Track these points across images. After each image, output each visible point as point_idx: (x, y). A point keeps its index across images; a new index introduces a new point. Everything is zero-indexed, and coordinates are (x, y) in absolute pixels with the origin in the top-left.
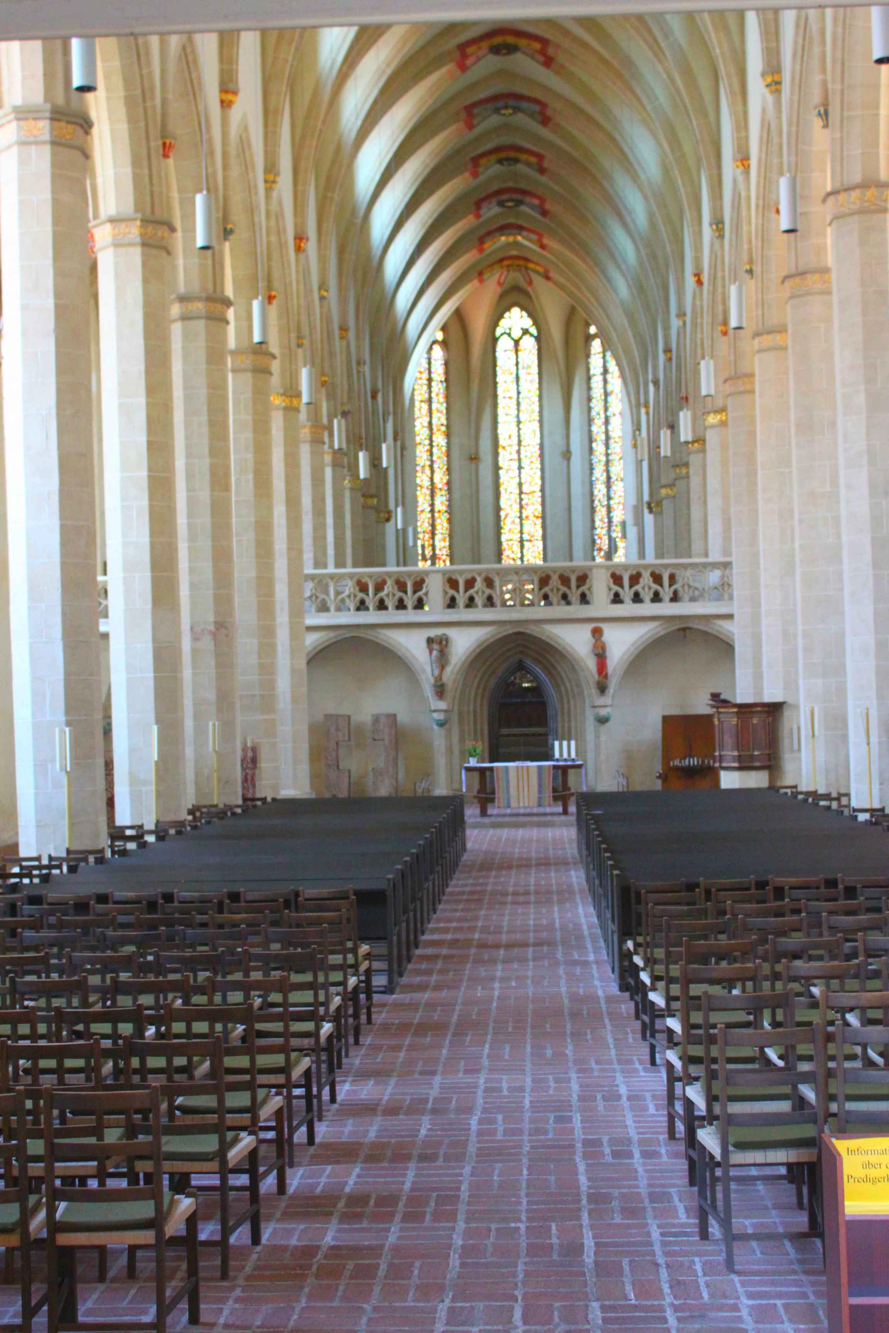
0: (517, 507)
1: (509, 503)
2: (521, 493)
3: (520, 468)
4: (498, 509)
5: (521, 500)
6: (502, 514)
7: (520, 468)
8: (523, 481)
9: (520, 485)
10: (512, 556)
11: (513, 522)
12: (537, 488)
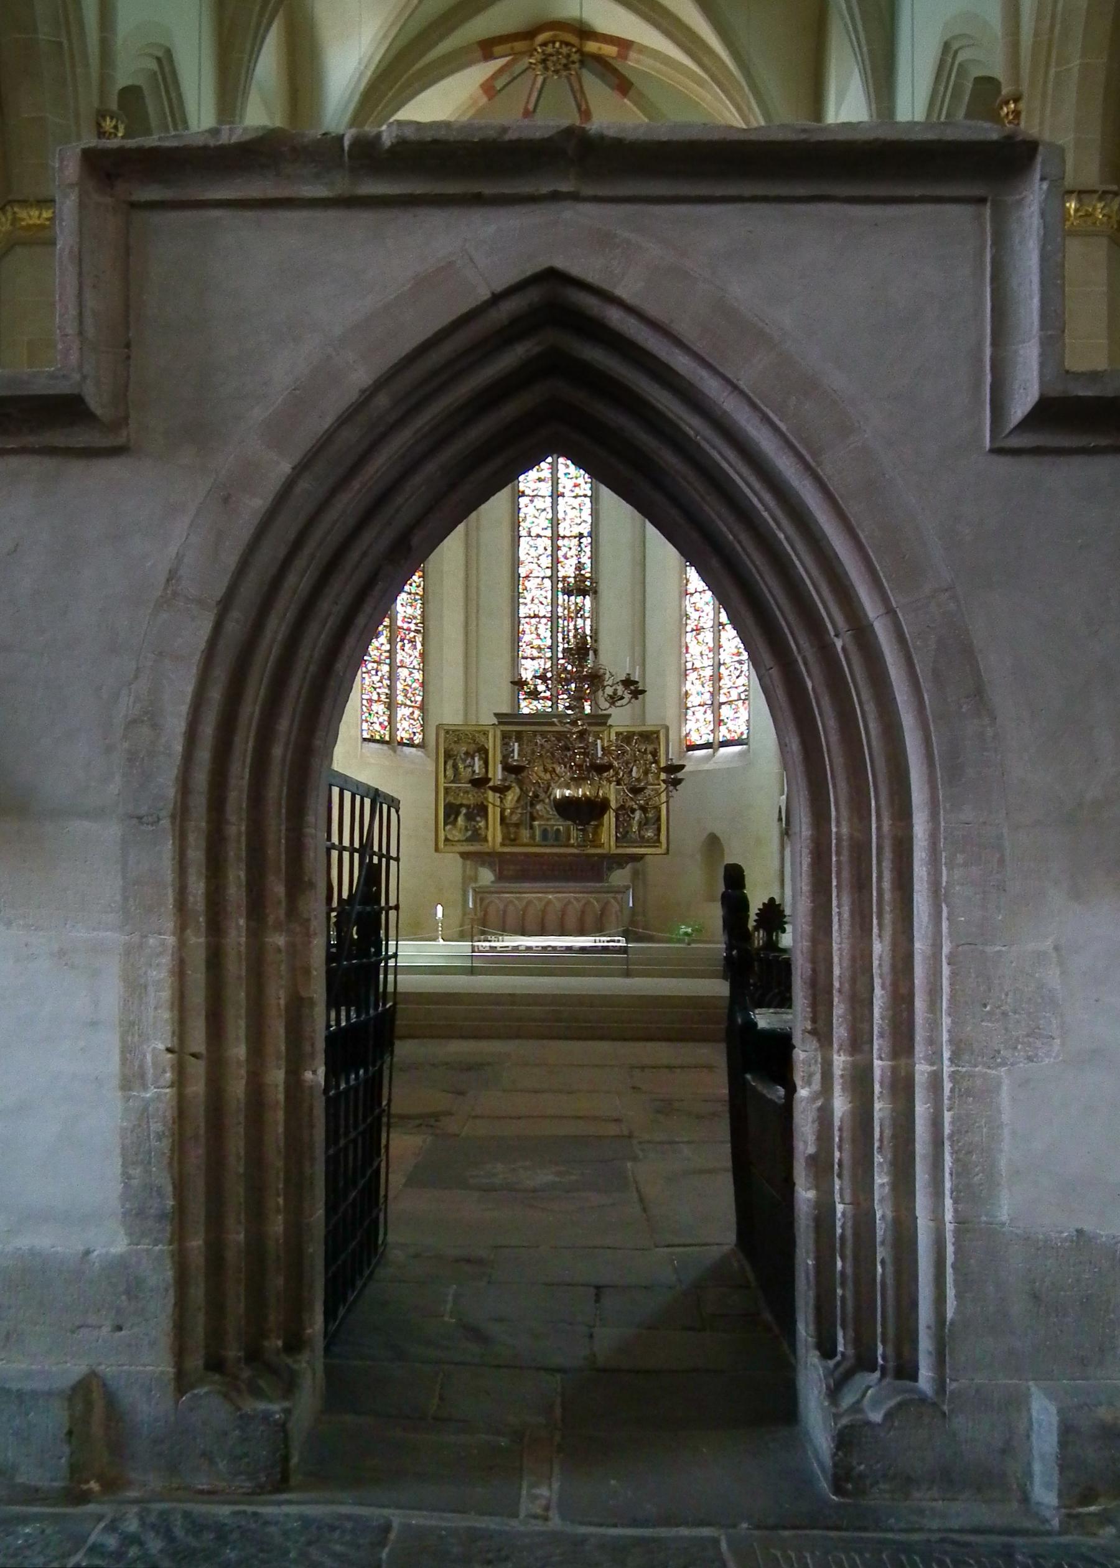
0: (546, 561)
1: (533, 553)
2: (555, 537)
3: (556, 495)
4: (516, 562)
5: (556, 548)
6: (523, 571)
7: (556, 495)
8: (561, 515)
9: (555, 523)
10: (536, 643)
11: (540, 587)
12: (585, 529)
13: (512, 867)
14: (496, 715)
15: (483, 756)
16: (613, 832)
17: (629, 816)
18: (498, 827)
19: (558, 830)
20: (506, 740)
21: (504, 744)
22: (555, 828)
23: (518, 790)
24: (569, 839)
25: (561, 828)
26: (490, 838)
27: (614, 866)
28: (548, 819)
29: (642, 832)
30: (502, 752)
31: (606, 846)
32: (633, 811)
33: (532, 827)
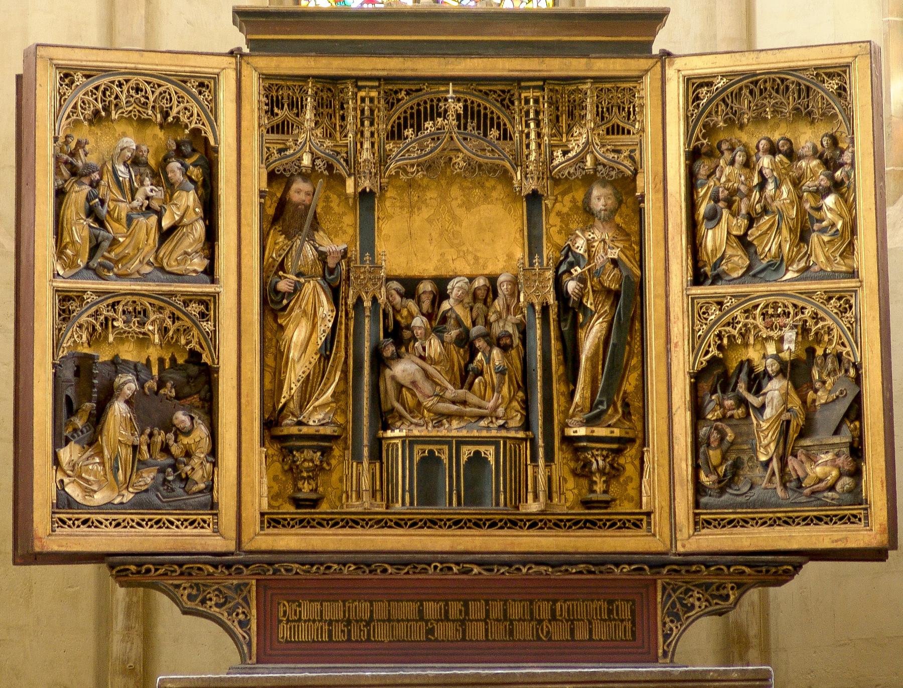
13: (308, 609)
14: (243, 17)
15: (196, 173)
16: (684, 467)
17: (742, 402)
18: (255, 453)
19: (477, 460)
20: (282, 113)
21: (272, 130)
22: (467, 452)
23: (326, 309)
24: (518, 498)
25: (489, 452)
26: (225, 496)
27: (695, 598)
28: (441, 418)
29: (792, 463)
30: (266, 159)
31: (660, 520)
32: (757, 382)
33: (378, 450)
